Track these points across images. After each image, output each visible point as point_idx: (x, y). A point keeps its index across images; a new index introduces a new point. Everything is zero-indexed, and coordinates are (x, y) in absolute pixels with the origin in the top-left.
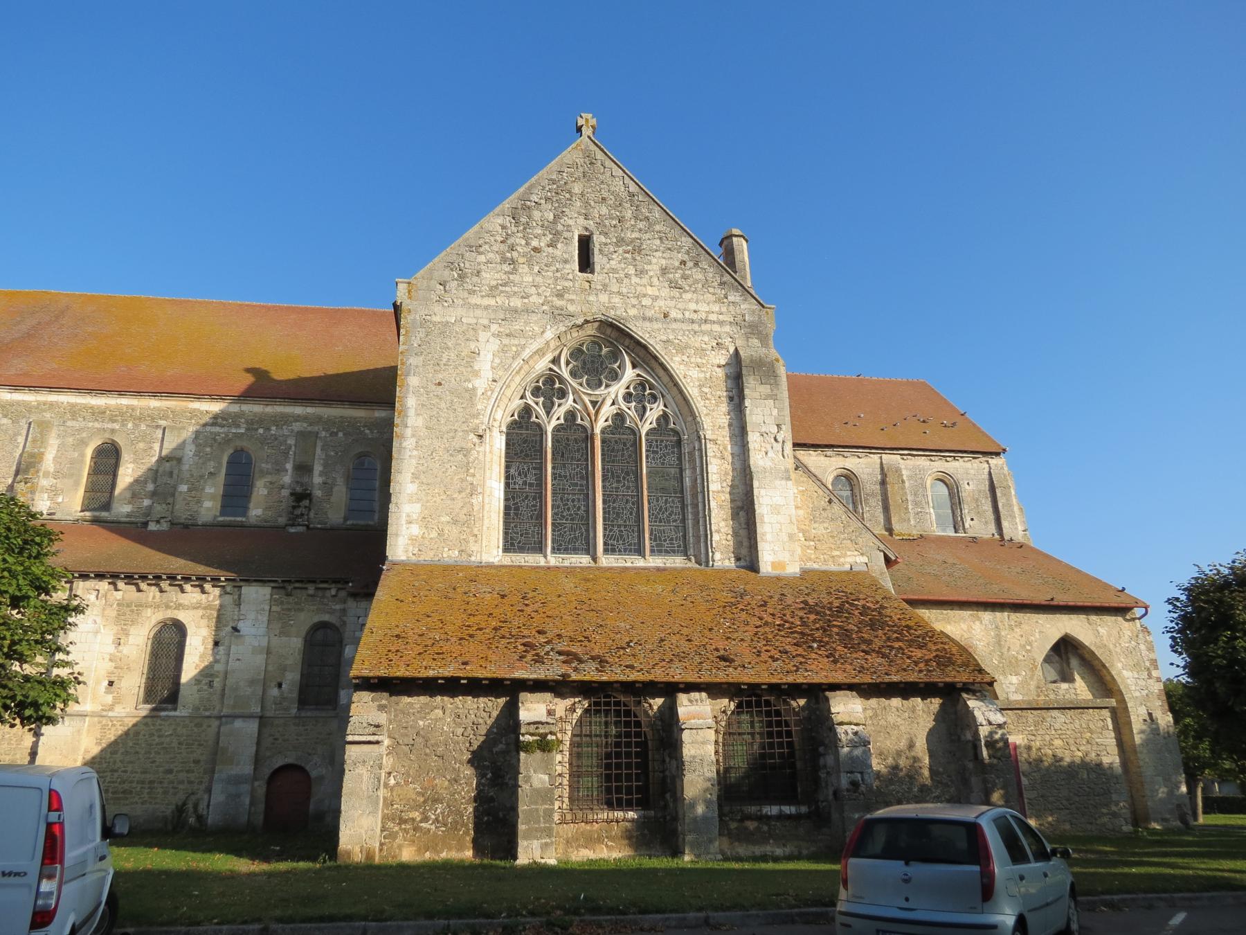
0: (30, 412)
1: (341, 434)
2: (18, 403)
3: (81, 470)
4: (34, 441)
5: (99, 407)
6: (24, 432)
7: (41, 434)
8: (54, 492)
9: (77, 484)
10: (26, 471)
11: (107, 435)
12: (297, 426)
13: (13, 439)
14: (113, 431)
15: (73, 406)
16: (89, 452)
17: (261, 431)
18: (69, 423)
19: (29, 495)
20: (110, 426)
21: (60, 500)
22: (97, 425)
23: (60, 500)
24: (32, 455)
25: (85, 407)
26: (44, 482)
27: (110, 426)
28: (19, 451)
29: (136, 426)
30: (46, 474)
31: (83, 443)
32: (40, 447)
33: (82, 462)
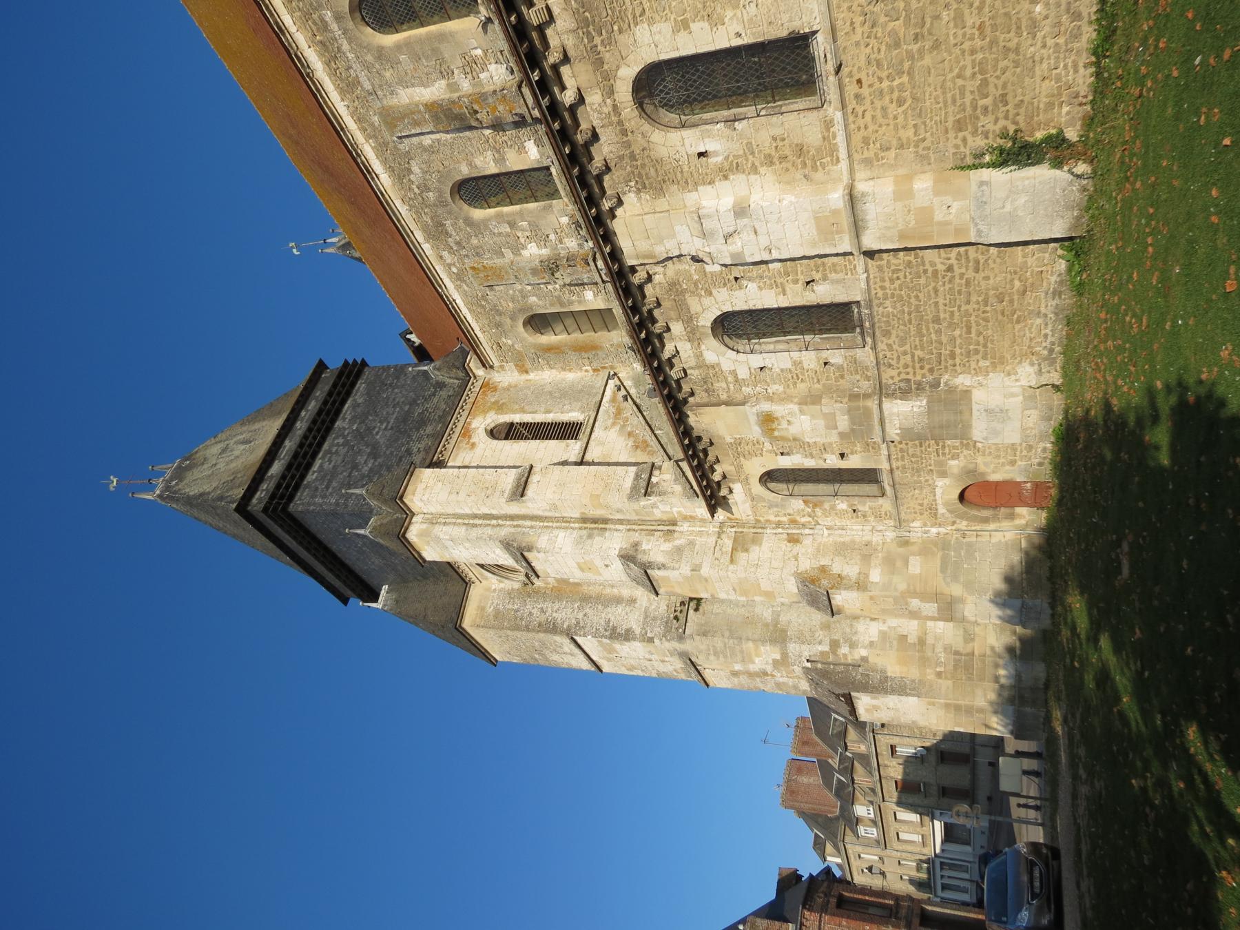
0: (386, 144)
2: (384, 162)
3: (420, 40)
4: (416, 123)
5: (321, 55)
6: (415, 140)
7: (403, 118)
8: (472, 66)
9: (442, 37)
10: (460, 117)
11: (350, 24)
13: (430, 150)
14: (338, 18)
15: (343, 93)
16: (389, 40)
18: (367, 86)
19: (490, 100)
20: (334, 26)
21: (479, 52)
22: (345, 47)
23: (479, 52)
24: (436, 118)
25: (334, 73)
26: (466, 86)
27: (334, 26)
28: (443, 136)
30: (453, 87)
31: (381, 54)
32: (419, 112)
33: (408, 44)
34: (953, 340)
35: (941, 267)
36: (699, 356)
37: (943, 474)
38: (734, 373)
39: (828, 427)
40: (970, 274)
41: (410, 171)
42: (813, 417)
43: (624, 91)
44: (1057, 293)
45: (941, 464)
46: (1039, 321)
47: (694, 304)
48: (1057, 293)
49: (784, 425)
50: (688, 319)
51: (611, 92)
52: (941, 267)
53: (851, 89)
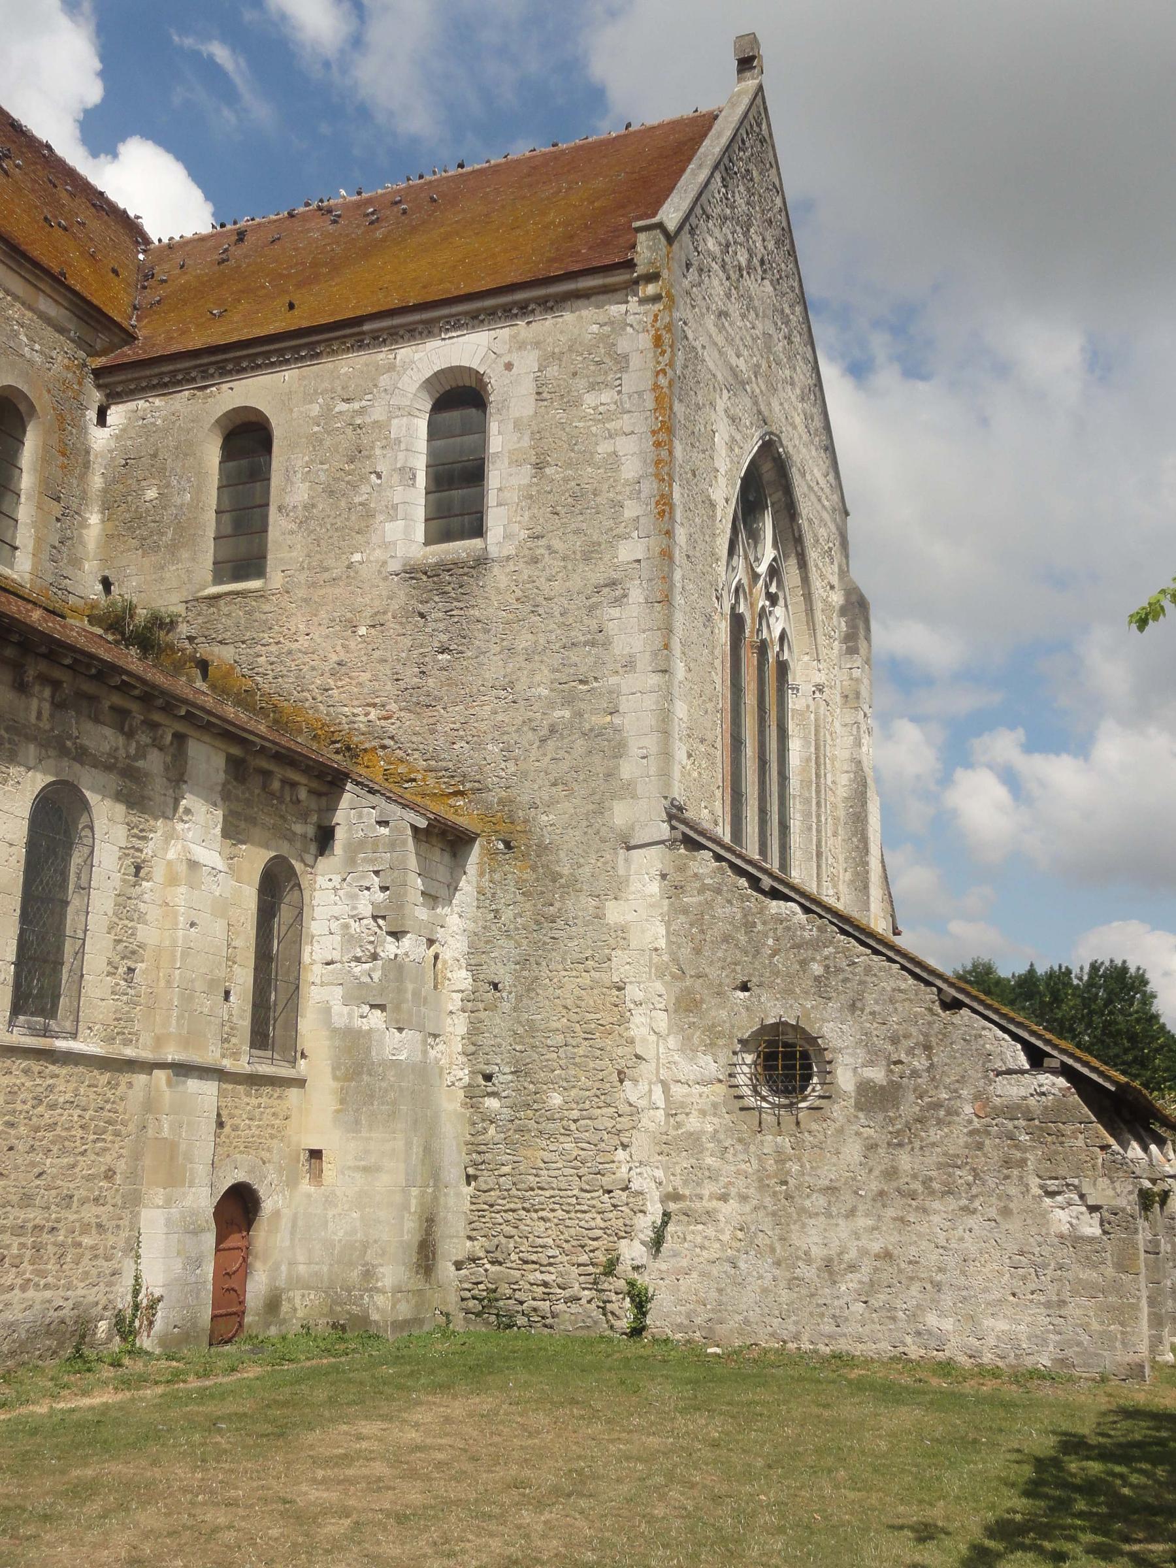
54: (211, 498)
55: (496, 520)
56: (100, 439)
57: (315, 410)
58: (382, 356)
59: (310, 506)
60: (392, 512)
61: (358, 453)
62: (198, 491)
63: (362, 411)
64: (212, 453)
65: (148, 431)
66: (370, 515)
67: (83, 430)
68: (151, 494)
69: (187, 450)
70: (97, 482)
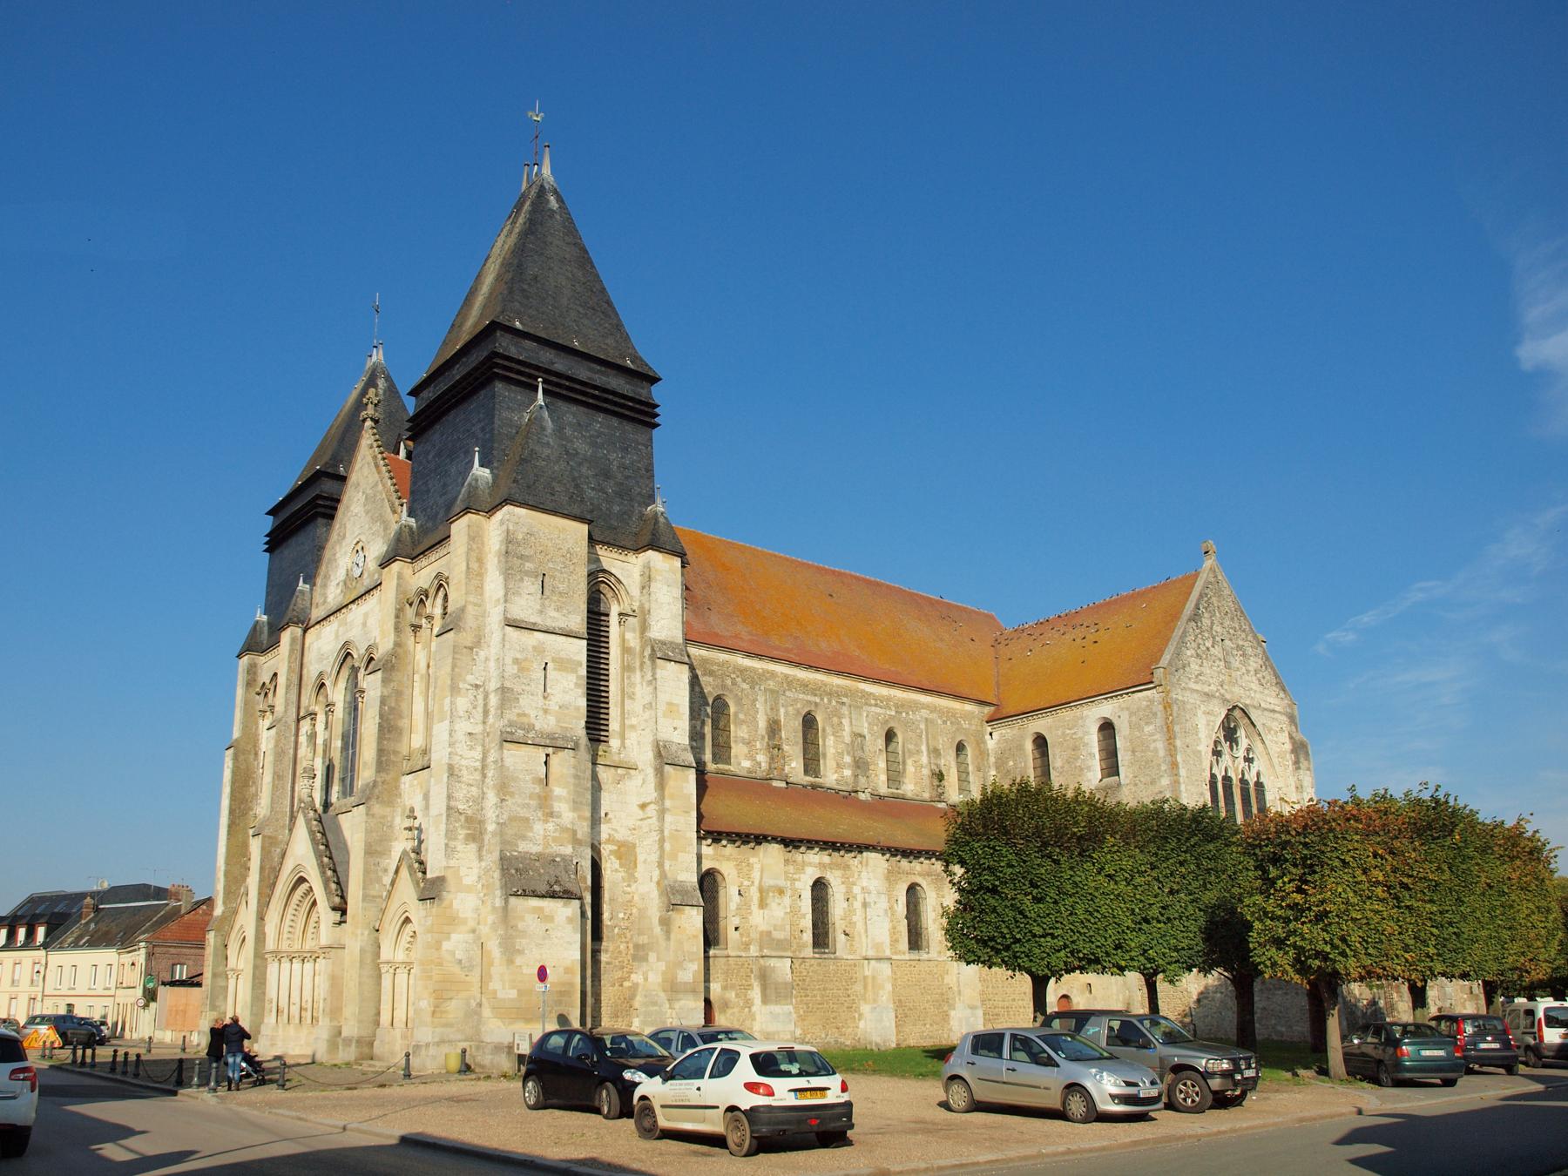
1: (948, 723)
12: (924, 713)
17: (904, 714)
29: (830, 701)
34: (815, 996)
35: (849, 992)
36: (810, 864)
37: (725, 988)
38: (799, 880)
39: (775, 926)
40: (846, 1004)
41: (744, 681)
42: (783, 919)
43: (919, 880)
44: (836, 1042)
45: (733, 987)
46: (823, 1036)
47: (838, 873)
48: (836, 1042)
49: (777, 900)
50: (832, 866)
51: (920, 874)
52: (849, 992)
53: (913, 963)
54: (1031, 763)
55: (1122, 770)
56: (991, 744)
57: (1060, 733)
58: (1076, 712)
59: (1062, 767)
60: (1089, 768)
61: (1075, 749)
62: (1025, 762)
63: (1075, 733)
64: (1029, 746)
65: (1006, 741)
66: (1082, 770)
67: (984, 742)
68: (1011, 763)
69: (1021, 748)
70: (992, 760)
